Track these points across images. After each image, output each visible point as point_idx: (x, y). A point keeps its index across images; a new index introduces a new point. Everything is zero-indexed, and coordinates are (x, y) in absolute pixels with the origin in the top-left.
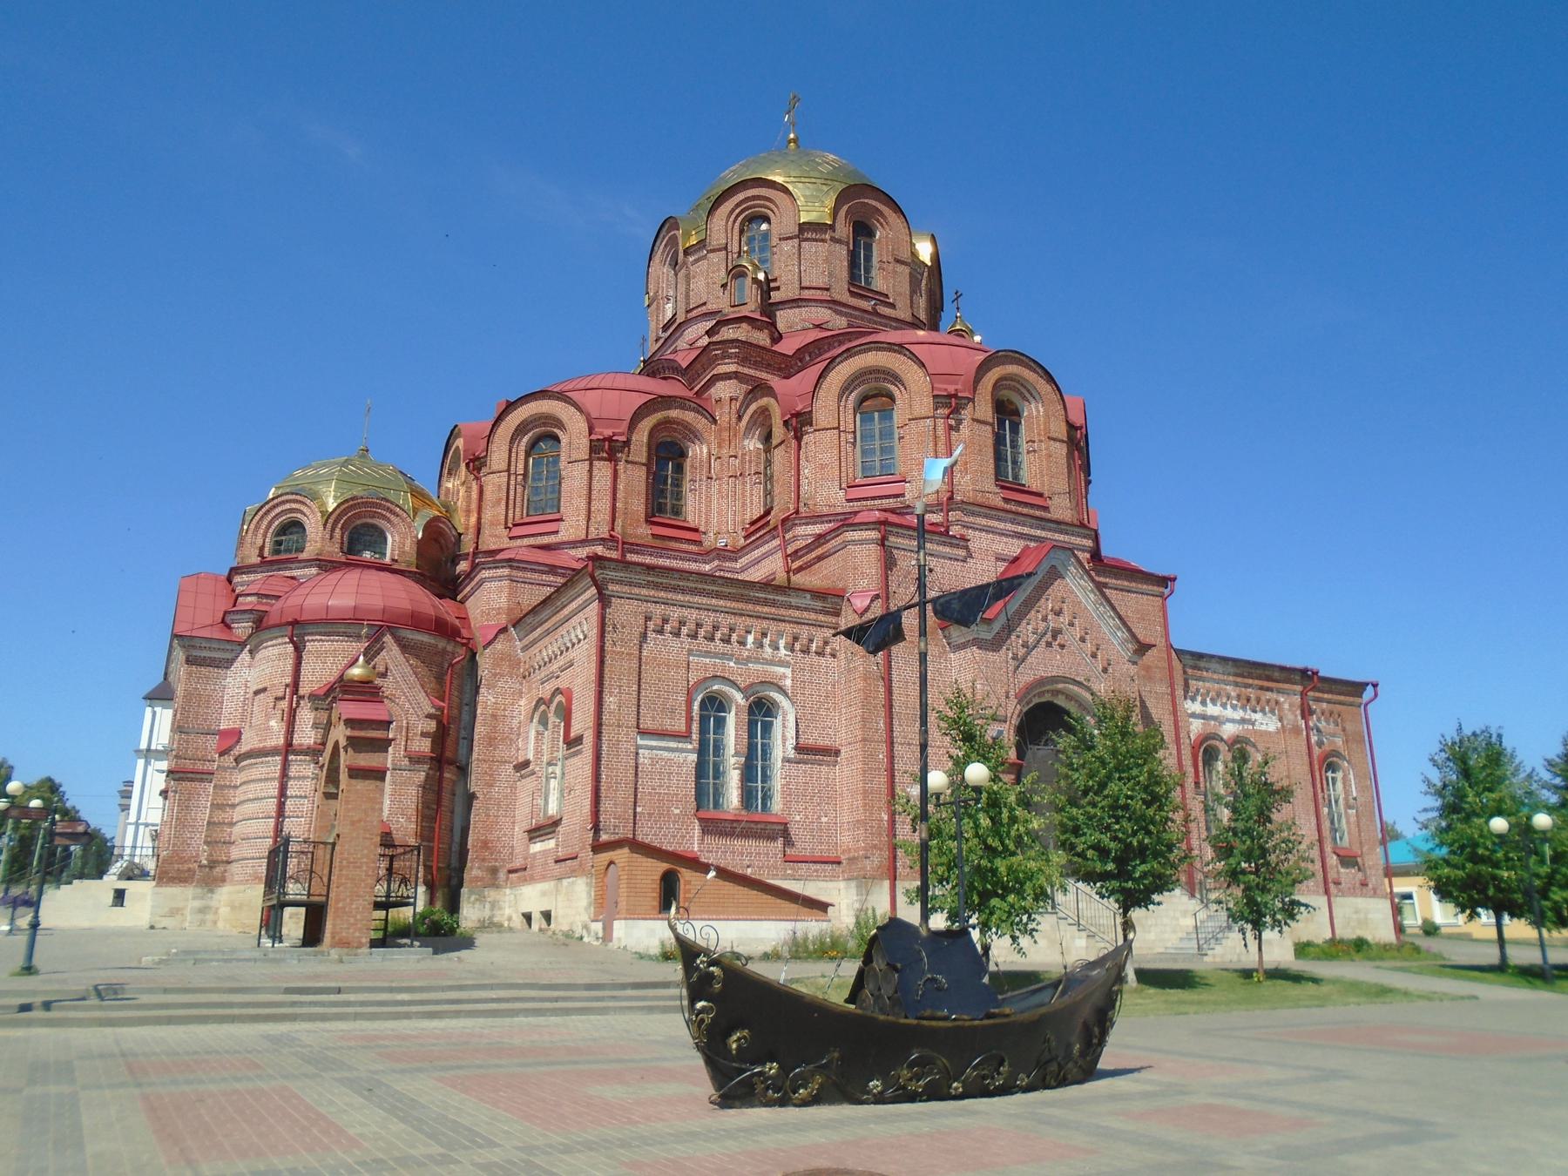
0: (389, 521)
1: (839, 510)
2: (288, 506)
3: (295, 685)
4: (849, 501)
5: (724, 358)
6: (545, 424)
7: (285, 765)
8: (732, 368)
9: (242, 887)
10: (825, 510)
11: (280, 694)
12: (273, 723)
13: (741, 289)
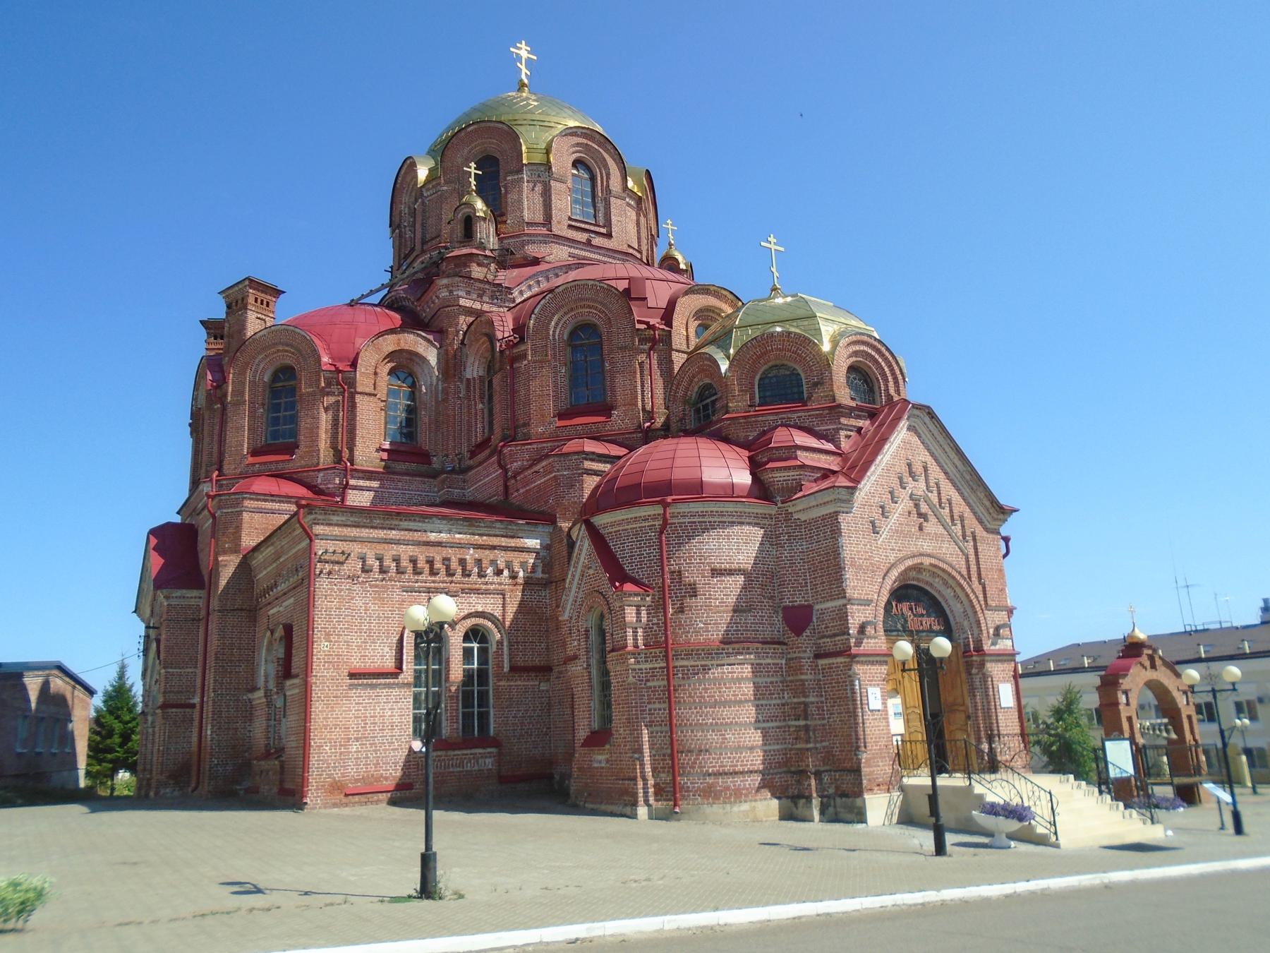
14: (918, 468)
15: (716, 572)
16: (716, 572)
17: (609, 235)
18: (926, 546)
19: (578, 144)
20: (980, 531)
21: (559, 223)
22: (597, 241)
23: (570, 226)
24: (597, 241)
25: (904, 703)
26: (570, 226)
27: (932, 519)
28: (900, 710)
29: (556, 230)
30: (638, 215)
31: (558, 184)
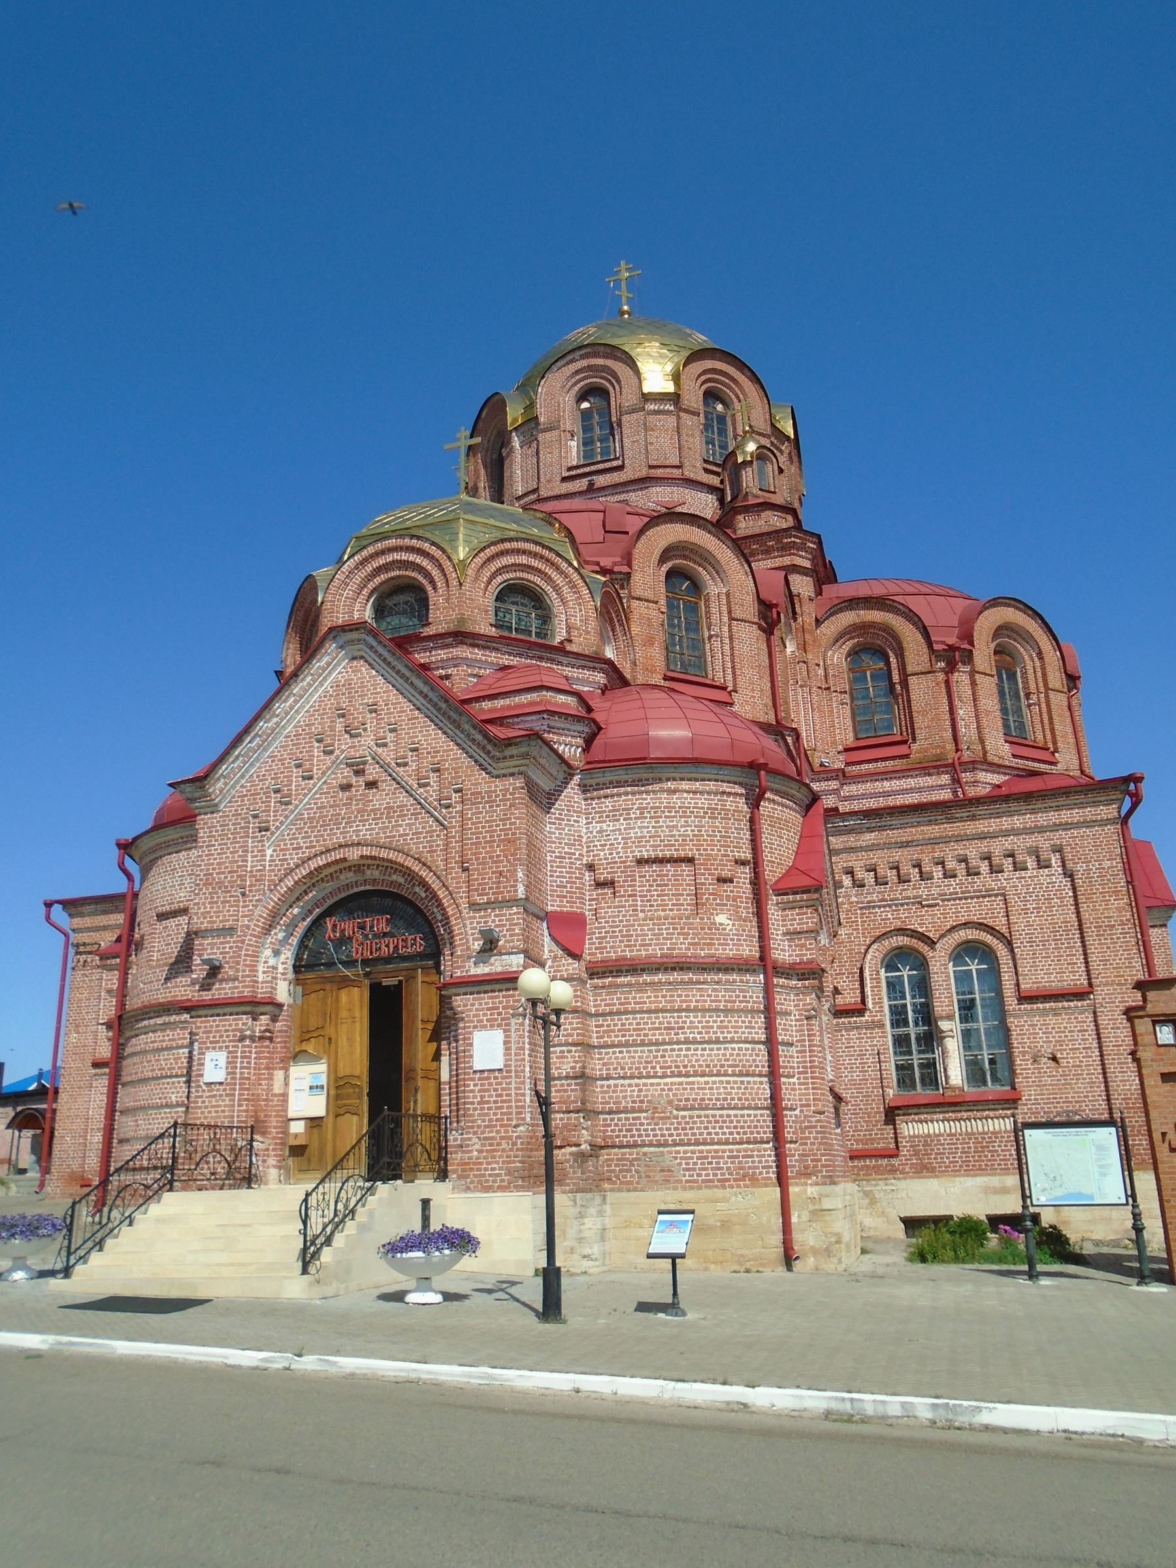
0: (613, 630)
1: (1007, 763)
2: (523, 560)
3: (756, 863)
4: (1014, 756)
5: (798, 549)
6: (685, 557)
7: (768, 990)
8: (807, 564)
9: (719, 1193)
10: (996, 760)
11: (726, 873)
12: (721, 919)
13: (761, 473)
14: (359, 712)
15: (162, 917)
16: (162, 917)
17: (621, 468)
18: (365, 832)
19: (577, 372)
20: (477, 781)
21: (549, 481)
22: (601, 481)
23: (564, 479)
24: (601, 481)
25: (333, 1070)
26: (564, 479)
27: (387, 786)
28: (323, 1080)
29: (544, 493)
30: (679, 418)
31: (547, 435)
